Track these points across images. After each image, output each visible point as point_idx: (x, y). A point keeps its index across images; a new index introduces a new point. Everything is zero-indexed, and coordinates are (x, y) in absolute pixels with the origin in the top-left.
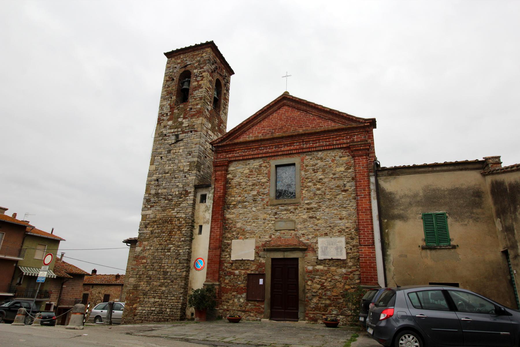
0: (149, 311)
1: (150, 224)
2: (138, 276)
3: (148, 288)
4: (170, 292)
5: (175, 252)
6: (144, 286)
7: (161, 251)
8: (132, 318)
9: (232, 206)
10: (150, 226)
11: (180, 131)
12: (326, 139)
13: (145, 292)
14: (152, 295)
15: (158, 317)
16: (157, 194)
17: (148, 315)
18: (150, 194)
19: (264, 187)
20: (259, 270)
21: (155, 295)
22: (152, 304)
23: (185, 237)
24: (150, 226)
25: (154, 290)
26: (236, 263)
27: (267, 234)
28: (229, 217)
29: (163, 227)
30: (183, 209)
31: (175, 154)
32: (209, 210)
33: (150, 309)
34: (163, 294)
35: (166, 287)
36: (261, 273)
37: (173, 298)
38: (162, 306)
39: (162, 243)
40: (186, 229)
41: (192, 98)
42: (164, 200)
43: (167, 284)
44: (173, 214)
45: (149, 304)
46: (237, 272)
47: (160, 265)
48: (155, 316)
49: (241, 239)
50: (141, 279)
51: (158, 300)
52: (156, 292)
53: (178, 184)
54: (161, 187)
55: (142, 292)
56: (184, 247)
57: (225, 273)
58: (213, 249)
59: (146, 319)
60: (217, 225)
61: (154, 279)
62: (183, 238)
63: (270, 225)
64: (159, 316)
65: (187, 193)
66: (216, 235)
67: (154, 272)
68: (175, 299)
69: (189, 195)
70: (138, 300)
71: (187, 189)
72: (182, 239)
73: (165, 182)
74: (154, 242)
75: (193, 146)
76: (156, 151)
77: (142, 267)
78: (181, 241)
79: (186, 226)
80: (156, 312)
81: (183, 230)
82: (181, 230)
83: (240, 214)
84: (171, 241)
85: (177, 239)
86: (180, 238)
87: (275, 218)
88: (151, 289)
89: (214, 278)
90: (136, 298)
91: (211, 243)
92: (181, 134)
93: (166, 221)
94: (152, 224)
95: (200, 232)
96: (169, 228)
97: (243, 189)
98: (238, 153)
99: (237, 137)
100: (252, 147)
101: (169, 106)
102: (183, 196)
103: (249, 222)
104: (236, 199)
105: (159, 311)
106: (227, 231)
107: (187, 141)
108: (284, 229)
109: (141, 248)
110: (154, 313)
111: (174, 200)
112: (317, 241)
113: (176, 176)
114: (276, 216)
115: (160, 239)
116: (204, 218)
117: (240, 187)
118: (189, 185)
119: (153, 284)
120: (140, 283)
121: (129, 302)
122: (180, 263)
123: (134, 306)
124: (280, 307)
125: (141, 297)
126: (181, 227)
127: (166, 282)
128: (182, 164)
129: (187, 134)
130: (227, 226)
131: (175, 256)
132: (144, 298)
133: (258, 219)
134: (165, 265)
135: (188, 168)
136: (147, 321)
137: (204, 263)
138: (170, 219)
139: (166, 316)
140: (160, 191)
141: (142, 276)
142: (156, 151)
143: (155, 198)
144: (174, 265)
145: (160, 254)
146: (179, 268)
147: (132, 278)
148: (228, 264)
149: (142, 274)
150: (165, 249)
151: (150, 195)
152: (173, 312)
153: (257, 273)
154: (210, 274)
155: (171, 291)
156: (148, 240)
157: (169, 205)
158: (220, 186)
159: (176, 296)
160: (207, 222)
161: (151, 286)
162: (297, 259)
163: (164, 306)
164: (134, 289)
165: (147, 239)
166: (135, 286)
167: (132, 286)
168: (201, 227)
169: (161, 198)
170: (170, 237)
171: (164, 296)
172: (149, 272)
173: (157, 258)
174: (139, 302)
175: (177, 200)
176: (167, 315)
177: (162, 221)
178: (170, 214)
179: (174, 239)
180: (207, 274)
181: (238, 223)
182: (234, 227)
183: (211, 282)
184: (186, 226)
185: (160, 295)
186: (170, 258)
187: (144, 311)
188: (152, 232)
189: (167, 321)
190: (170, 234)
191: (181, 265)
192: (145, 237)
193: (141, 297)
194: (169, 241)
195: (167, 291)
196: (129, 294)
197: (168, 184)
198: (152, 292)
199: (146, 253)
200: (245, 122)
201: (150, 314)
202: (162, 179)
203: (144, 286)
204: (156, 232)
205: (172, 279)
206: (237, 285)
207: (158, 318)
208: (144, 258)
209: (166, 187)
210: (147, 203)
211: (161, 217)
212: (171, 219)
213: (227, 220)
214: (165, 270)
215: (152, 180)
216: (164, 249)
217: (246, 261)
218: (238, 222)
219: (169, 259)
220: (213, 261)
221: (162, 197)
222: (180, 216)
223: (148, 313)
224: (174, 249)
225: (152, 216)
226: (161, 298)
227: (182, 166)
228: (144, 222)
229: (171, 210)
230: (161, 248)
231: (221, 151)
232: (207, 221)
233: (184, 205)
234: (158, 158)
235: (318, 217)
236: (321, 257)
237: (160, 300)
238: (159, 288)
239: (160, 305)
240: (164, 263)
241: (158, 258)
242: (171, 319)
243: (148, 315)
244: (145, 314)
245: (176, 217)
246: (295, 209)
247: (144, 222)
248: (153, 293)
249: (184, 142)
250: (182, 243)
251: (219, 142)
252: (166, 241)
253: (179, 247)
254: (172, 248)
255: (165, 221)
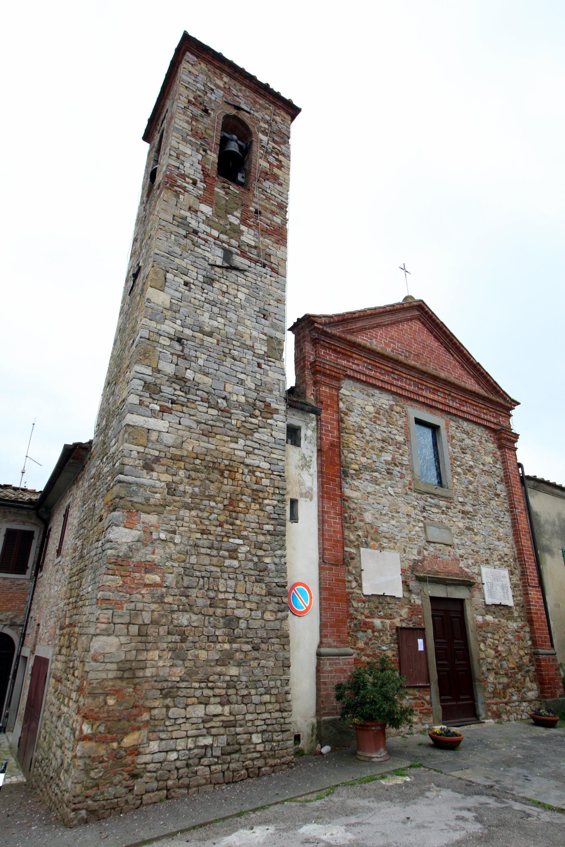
0: (190, 750)
1: (163, 461)
2: (134, 629)
3: (179, 671)
4: (255, 683)
5: (251, 560)
6: (161, 663)
7: (209, 551)
8: (123, 790)
9: (354, 472)
10: (164, 468)
11: (235, 247)
12: (474, 405)
13: (170, 684)
14: (198, 693)
15: (225, 767)
16: (180, 379)
17: (188, 766)
18: (159, 371)
19: (401, 451)
20: (414, 619)
21: (207, 692)
22: (201, 726)
23: (273, 522)
24: (164, 468)
25: (200, 676)
26: (369, 601)
27: (415, 546)
28: (351, 495)
29: (207, 482)
30: (263, 448)
31: (226, 295)
32: (309, 467)
33: (195, 742)
34: (235, 687)
35: (239, 665)
36: (417, 626)
37: (267, 698)
38: (234, 726)
39: (209, 528)
40: (275, 503)
41: (260, 190)
42: (206, 405)
43: (242, 656)
44: (237, 452)
45: (187, 726)
46: (377, 622)
47: (212, 594)
48: (217, 763)
49: (373, 547)
50: (151, 639)
51: (218, 709)
52: (210, 685)
53: (243, 376)
54: (193, 364)
55: (160, 686)
56: (274, 551)
57: (355, 625)
58: (332, 564)
59: (185, 781)
60: (334, 507)
61: (197, 639)
62: (267, 524)
63: (417, 529)
64: (229, 763)
65: (268, 411)
66: (334, 531)
67: (194, 617)
68: (273, 700)
69: (275, 416)
70: (146, 716)
71: (268, 400)
72: (266, 527)
73: (204, 357)
74: (183, 520)
75: (272, 302)
76: (168, 258)
77: (148, 598)
78: (264, 532)
79: (274, 494)
80: (218, 752)
81: (266, 502)
82: (260, 500)
83: (368, 493)
84: (236, 528)
85: (253, 525)
86: (260, 525)
87: (424, 517)
88: (190, 674)
89: (339, 636)
90: (135, 711)
91: (327, 549)
92: (237, 254)
93: (213, 467)
94: (170, 463)
95: (294, 518)
96: (225, 488)
97: (368, 442)
98: (358, 365)
99: (351, 332)
100: (382, 366)
101: (200, 167)
102: (257, 412)
103: (385, 515)
104: (358, 458)
105: (228, 744)
106: (347, 525)
107: (254, 281)
108: (439, 541)
109: (135, 534)
110: (212, 756)
111: (237, 417)
112: (480, 570)
113: (236, 353)
114: (425, 514)
115: (200, 514)
116: (301, 483)
117: (363, 437)
118: (271, 391)
119: (197, 656)
120: (145, 653)
121: (102, 729)
122: (269, 594)
123: (129, 741)
124: (449, 697)
125: (156, 704)
126: (261, 495)
127: (236, 651)
128: (248, 332)
129: (253, 265)
130: (346, 515)
131: (252, 572)
132: (168, 707)
133: (399, 512)
134: (230, 596)
135: (265, 349)
136: (188, 787)
137: (311, 598)
138: (227, 462)
139: (252, 760)
140: (189, 375)
141: (151, 630)
142: (168, 258)
143: (175, 390)
144: (254, 598)
145: (207, 560)
146: (270, 607)
147: (109, 635)
148: (360, 604)
149: (152, 622)
150: (221, 549)
151: (159, 376)
152: (272, 741)
153: (411, 626)
154: (331, 626)
155: (257, 678)
156: (160, 509)
157: (222, 425)
158: (333, 420)
159: (274, 691)
160: (307, 495)
161: (188, 664)
162: (461, 602)
163: (241, 726)
164: (121, 678)
165: (155, 505)
166: (128, 665)
167: (114, 666)
168: (294, 502)
169: (196, 395)
170: (234, 515)
171: (237, 694)
172: (175, 616)
173: (198, 574)
174: (147, 723)
175: (243, 419)
176: (255, 755)
177: (204, 463)
178: (227, 450)
179: (245, 524)
180: (323, 626)
181: (367, 513)
182: (361, 521)
183: (336, 647)
184: (274, 494)
185: (223, 692)
186: (241, 577)
187: (173, 756)
188: (171, 489)
189: (258, 775)
190: (231, 508)
191: (275, 600)
192: (147, 499)
193: (156, 704)
194: (231, 527)
195: (244, 679)
196: (101, 698)
197: (216, 366)
198: (197, 685)
199: (153, 553)
200: (369, 312)
201: (197, 761)
202: (193, 343)
203: (161, 663)
204: (185, 492)
205: (256, 641)
206: (381, 653)
207: (228, 768)
208: (150, 567)
209: (207, 370)
210: (147, 395)
211: (197, 450)
212: (229, 465)
213: (347, 501)
214: (229, 612)
215: (160, 332)
216: (219, 549)
217: (388, 598)
218: (366, 510)
219: (236, 579)
220: (335, 595)
221: (198, 392)
222: (256, 463)
223: (189, 758)
224: (249, 552)
225: (169, 439)
226: (229, 703)
227: (248, 336)
228: (141, 449)
229: (229, 439)
230: (206, 543)
231: (327, 345)
232: (308, 491)
233: (265, 438)
234: (177, 279)
235: (476, 530)
236: (489, 601)
237: (227, 708)
238: (219, 669)
239: (226, 725)
240: (226, 592)
241: (204, 574)
242: (271, 766)
243: (188, 766)
244: (178, 764)
245: (243, 463)
246: (448, 508)
247: (141, 449)
248: (200, 688)
249: (249, 279)
250: (269, 537)
251: (325, 324)
252: (221, 525)
253: (260, 549)
254: (244, 549)
255: (211, 465)
